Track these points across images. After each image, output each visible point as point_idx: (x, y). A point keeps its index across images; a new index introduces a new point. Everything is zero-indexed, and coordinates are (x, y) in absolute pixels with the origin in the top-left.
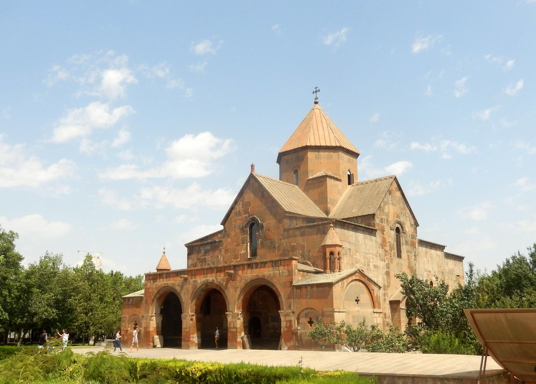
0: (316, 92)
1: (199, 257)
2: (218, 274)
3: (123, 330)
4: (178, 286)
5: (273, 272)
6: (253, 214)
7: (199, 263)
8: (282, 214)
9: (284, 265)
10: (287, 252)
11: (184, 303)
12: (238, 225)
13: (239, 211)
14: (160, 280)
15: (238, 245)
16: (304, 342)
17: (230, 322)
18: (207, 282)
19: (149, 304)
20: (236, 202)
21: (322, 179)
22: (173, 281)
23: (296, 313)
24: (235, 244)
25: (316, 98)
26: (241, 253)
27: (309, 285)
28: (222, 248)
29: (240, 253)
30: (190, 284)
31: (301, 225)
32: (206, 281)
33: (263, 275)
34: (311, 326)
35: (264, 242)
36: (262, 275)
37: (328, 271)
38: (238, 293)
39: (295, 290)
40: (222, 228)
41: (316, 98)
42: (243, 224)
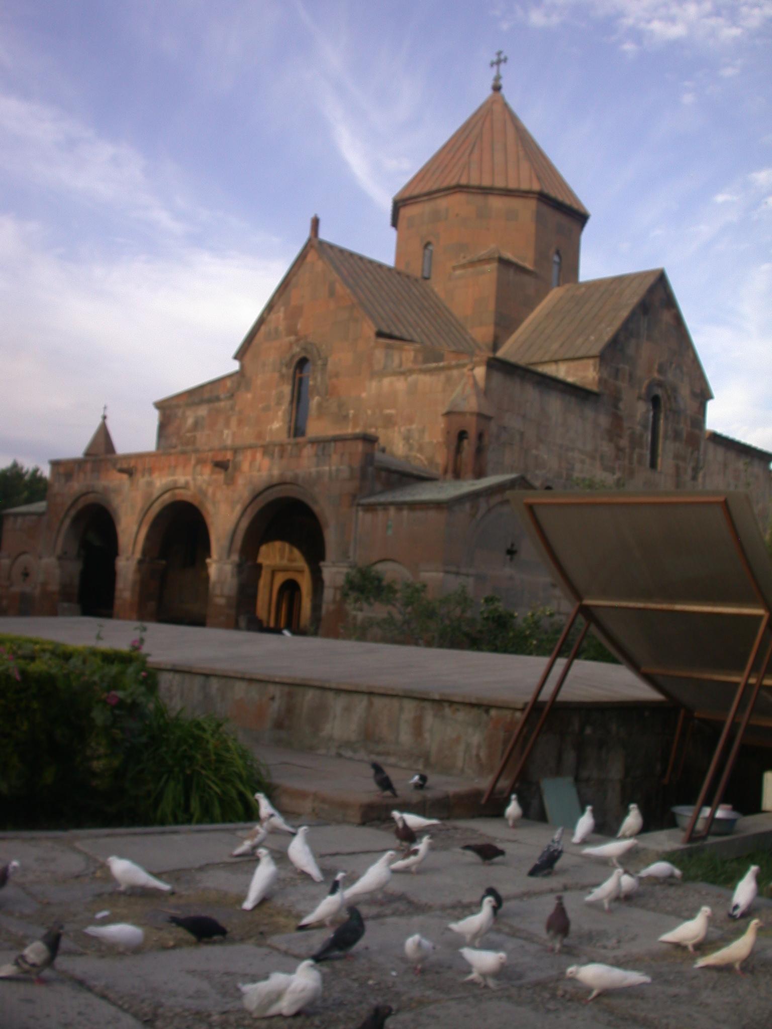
0: (498, 62)
2: (199, 468)
13: (276, 330)
15: (267, 409)
20: (270, 307)
24: (260, 406)
25: (498, 78)
27: (392, 504)
29: (269, 427)
37: (449, 475)
40: (235, 366)
41: (498, 78)
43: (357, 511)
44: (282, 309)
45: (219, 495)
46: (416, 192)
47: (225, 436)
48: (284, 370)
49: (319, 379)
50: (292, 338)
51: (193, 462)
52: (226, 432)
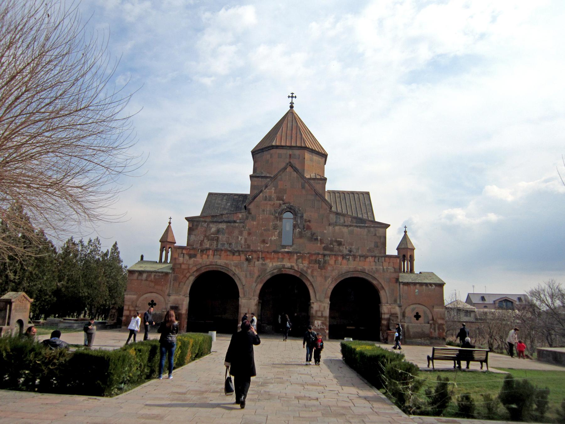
0: (292, 97)
1: (207, 235)
2: (300, 260)
3: (128, 310)
4: (234, 266)
5: (375, 267)
6: (289, 203)
7: (207, 241)
8: (327, 209)
9: (389, 261)
10: (332, 246)
11: (244, 286)
12: (268, 209)
14: (202, 256)
15: (269, 230)
16: (411, 333)
17: (316, 311)
18: (282, 266)
19: (181, 284)
21: (320, 181)
22: (227, 260)
23: (402, 307)
25: (292, 103)
26: (271, 239)
27: (419, 283)
28: (244, 230)
30: (254, 267)
31: (349, 223)
32: (281, 266)
33: (364, 268)
34: (417, 319)
35: (303, 233)
36: (361, 268)
38: (329, 282)
39: (401, 286)
41: (292, 103)
42: (274, 211)
43: (400, 285)
44: (273, 188)
45: (315, 273)
46: (283, 144)
47: (240, 239)
48: (277, 215)
49: (299, 221)
50: (281, 202)
51: (295, 257)
52: (240, 237)
